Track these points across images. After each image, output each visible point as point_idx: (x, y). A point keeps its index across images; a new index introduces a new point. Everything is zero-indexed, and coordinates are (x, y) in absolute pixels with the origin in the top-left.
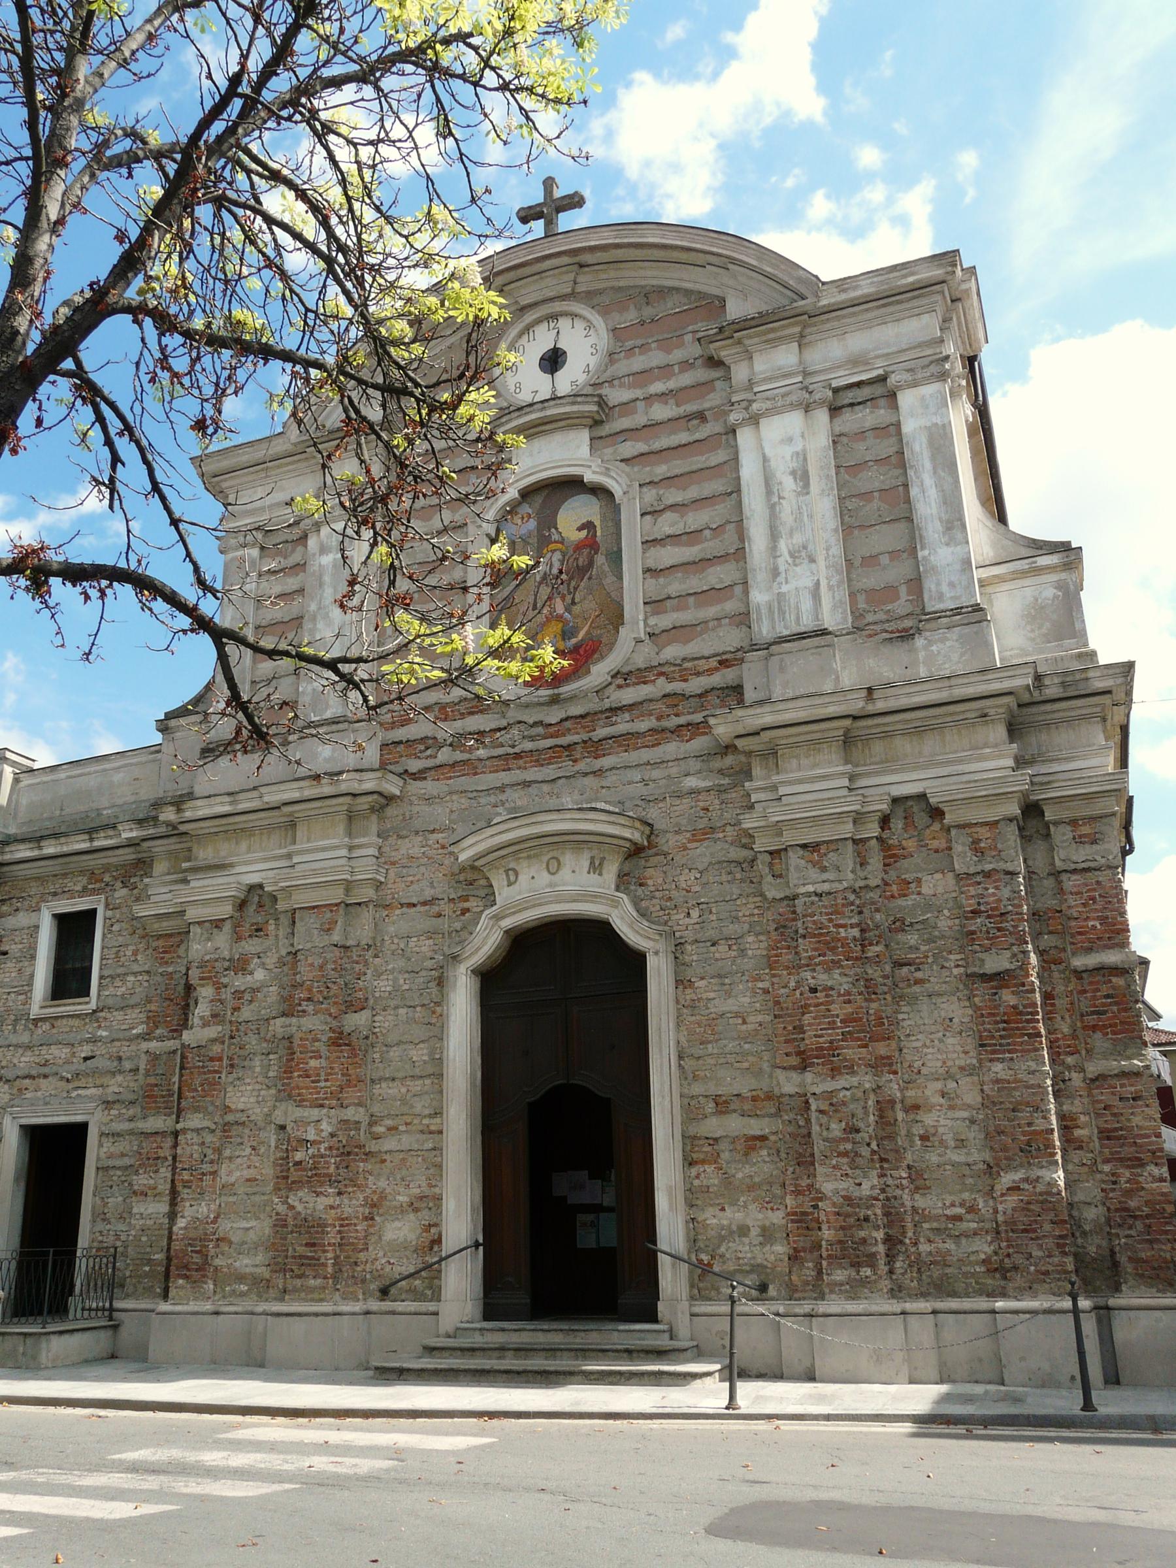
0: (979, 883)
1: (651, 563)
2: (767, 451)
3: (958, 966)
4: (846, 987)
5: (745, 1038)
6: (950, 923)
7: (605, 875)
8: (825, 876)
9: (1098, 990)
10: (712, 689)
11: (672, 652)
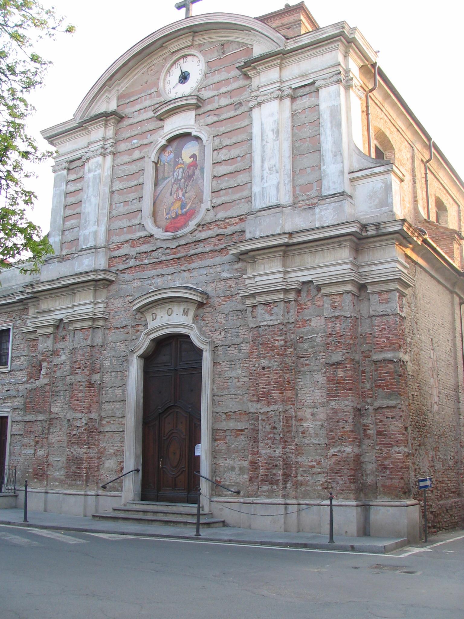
0: (333, 321)
1: (215, 174)
2: (263, 120)
3: (323, 358)
4: (275, 367)
5: (239, 388)
6: (321, 339)
7: (189, 317)
8: (272, 318)
9: (382, 370)
10: (236, 232)
11: (221, 215)
